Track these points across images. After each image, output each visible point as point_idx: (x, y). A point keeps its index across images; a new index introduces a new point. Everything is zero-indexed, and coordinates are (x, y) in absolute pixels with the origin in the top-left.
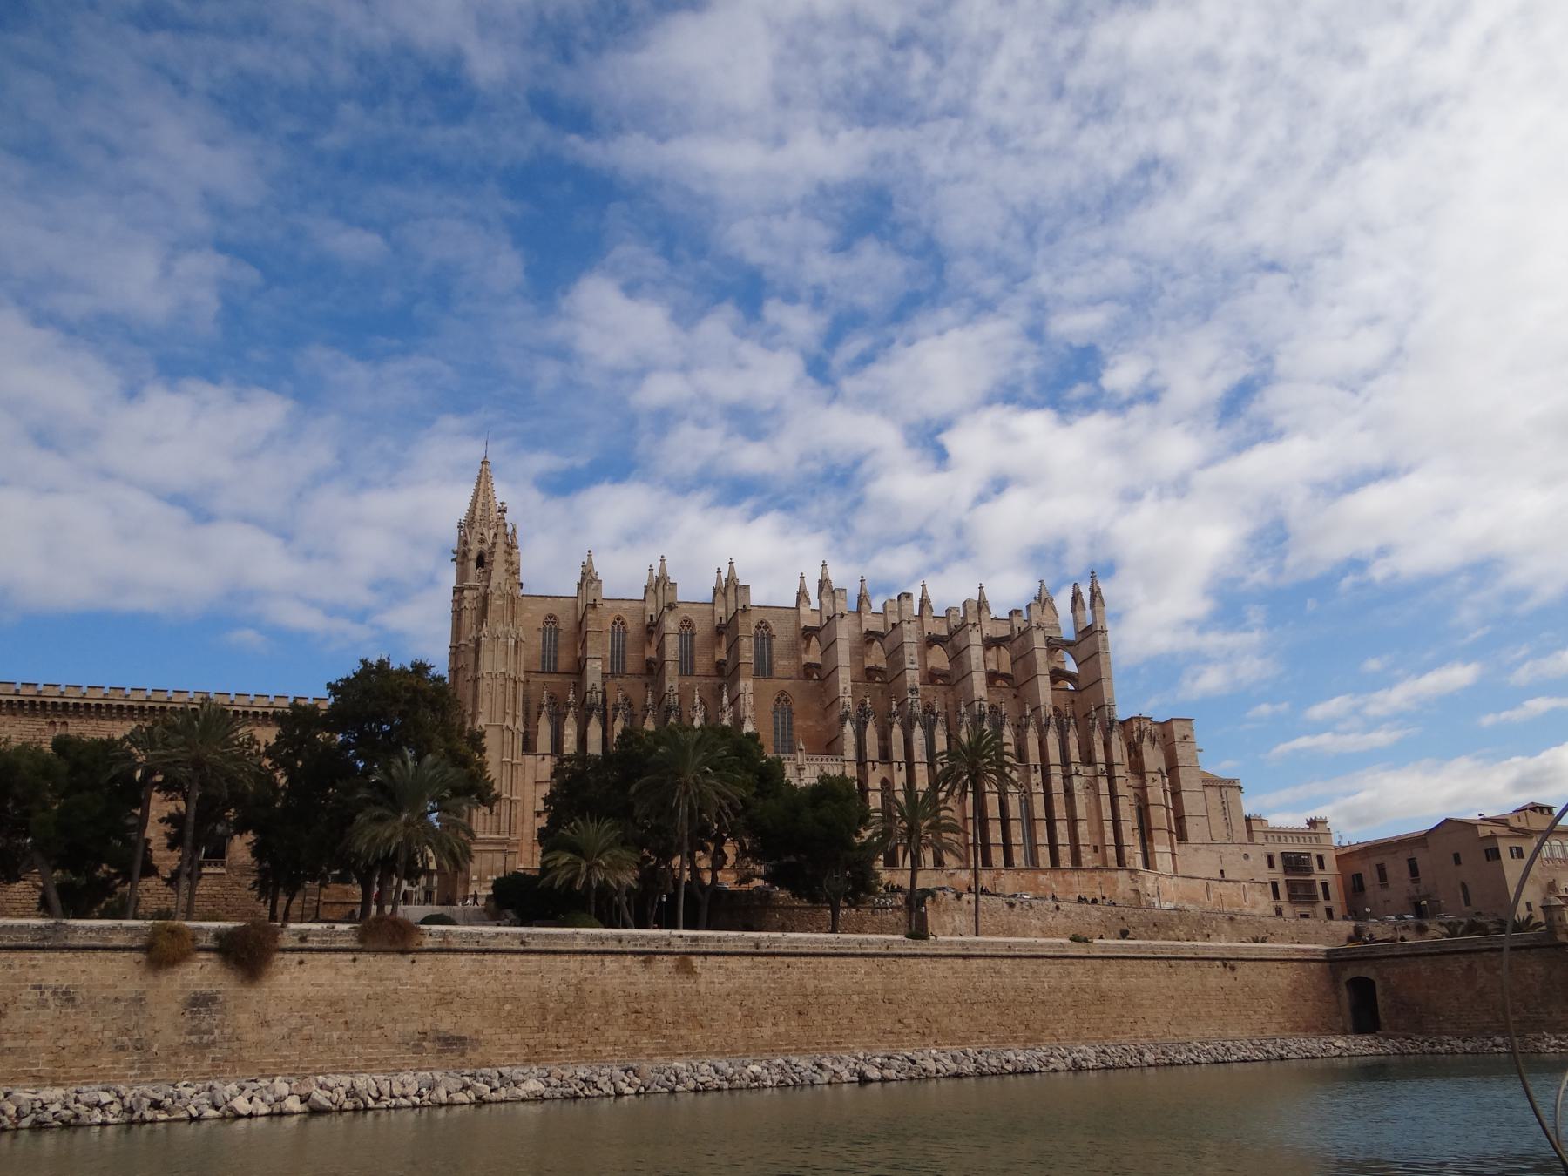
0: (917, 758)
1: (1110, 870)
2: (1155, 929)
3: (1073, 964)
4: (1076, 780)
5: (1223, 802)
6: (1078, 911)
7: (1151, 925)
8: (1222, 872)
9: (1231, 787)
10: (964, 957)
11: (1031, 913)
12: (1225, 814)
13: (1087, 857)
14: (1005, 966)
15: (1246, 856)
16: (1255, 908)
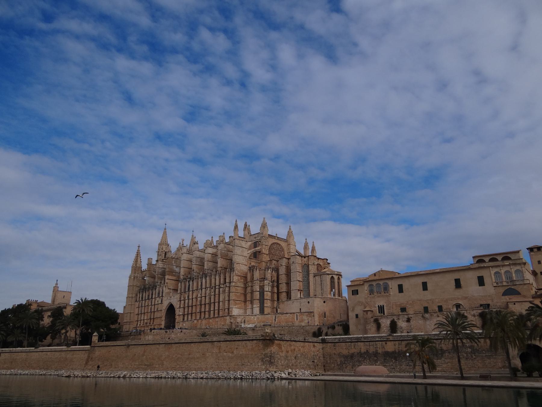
0: (190, 290)
1: (225, 316)
2: (218, 335)
3: (63, 352)
4: (221, 289)
5: (321, 281)
6: (189, 331)
7: (216, 334)
8: (300, 309)
9: (324, 274)
10: (42, 352)
11: (173, 333)
12: (321, 285)
13: (221, 313)
14: (49, 353)
15: (309, 302)
16: (302, 322)
